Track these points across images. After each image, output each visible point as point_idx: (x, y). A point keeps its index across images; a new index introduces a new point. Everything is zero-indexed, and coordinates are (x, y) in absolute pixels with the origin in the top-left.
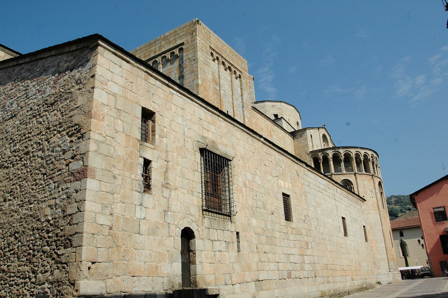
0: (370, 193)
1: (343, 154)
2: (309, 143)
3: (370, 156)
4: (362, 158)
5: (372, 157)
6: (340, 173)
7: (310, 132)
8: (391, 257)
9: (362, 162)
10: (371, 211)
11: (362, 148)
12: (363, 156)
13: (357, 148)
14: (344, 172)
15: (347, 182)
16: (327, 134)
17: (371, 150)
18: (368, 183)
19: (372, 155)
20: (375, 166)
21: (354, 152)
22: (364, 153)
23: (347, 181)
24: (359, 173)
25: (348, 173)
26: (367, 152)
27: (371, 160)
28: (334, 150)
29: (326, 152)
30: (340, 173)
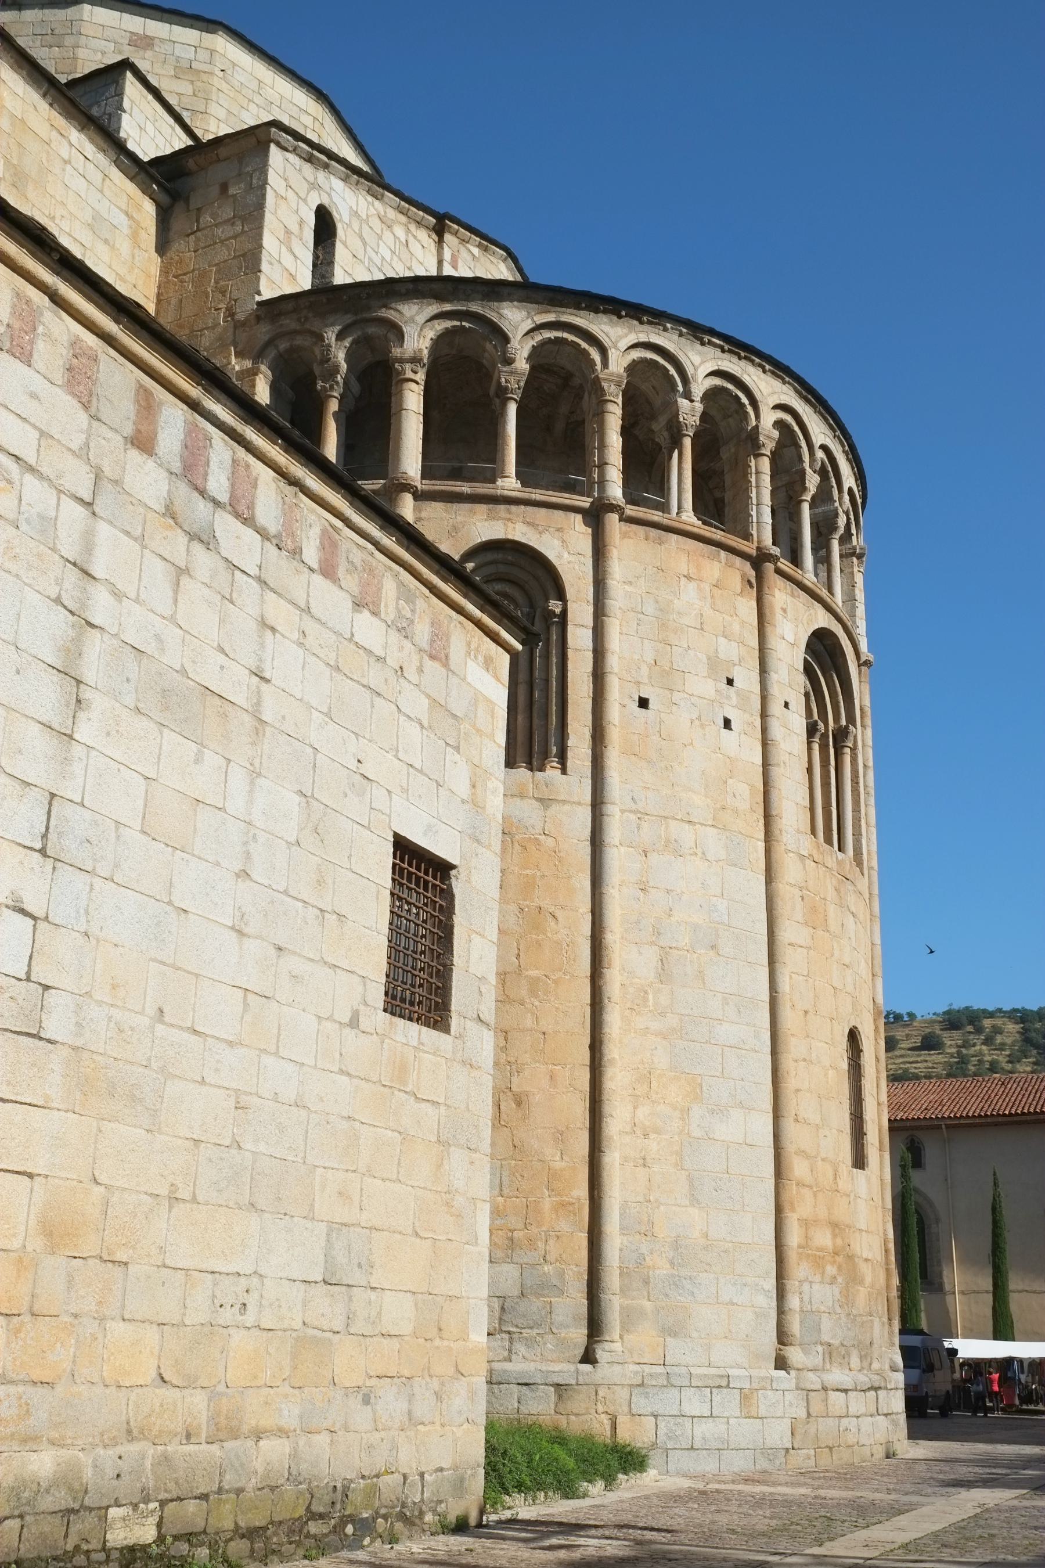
0: (709, 687)
1: (521, 351)
2: (269, 241)
7: (314, 186)
8: (824, 1239)
10: (686, 835)
11: (698, 331)
13: (657, 317)
14: (509, 483)
17: (781, 370)
18: (708, 611)
21: (624, 344)
22: (717, 381)
24: (631, 511)
25: (537, 495)
29: (384, 313)
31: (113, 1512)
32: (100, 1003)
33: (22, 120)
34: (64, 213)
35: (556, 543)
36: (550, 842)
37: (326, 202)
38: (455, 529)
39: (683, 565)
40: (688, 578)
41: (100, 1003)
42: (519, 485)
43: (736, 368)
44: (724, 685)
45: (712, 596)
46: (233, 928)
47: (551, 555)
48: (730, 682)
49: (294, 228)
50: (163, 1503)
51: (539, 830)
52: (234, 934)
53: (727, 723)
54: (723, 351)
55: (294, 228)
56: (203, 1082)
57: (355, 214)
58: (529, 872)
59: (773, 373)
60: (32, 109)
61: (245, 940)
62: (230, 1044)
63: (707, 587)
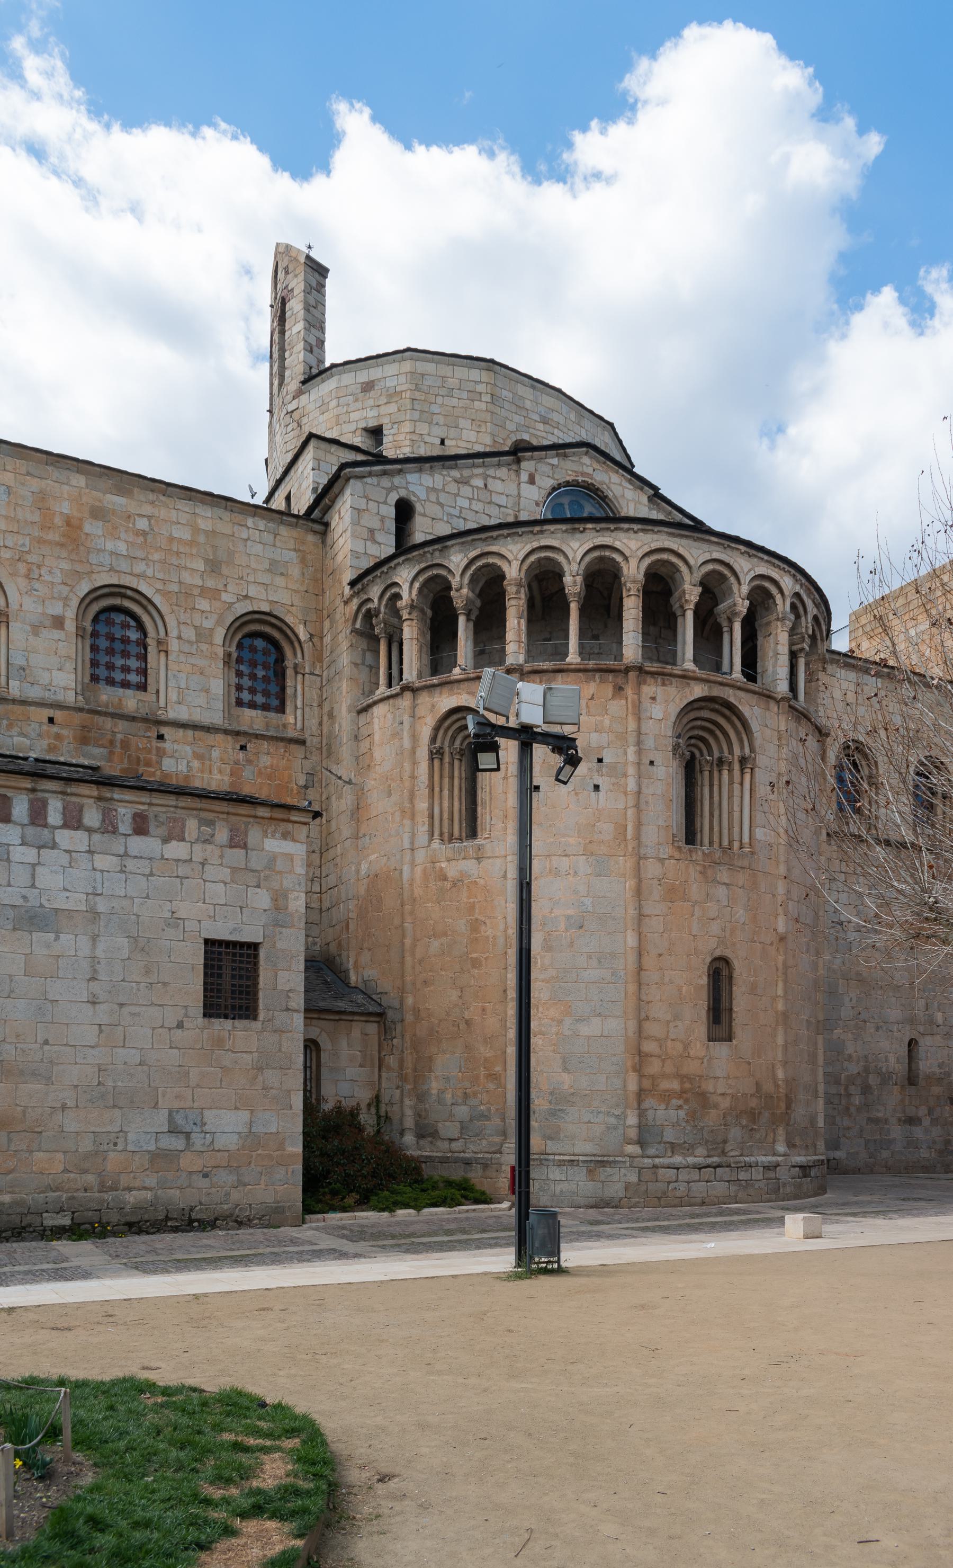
7: (394, 488)
26: (618, 544)
31: (45, 1215)
32: (10, 1043)
33: (213, 531)
34: (249, 571)
36: (481, 882)
37: (403, 493)
38: (433, 706)
41: (10, 1043)
43: (608, 539)
45: (588, 707)
46: (88, 1002)
48: (600, 760)
49: (376, 524)
50: (73, 1213)
51: (476, 875)
52: (89, 1005)
53: (597, 788)
54: (597, 531)
56: (76, 1063)
58: (472, 900)
59: (643, 530)
60: (219, 521)
61: (97, 1006)
62: (92, 1047)
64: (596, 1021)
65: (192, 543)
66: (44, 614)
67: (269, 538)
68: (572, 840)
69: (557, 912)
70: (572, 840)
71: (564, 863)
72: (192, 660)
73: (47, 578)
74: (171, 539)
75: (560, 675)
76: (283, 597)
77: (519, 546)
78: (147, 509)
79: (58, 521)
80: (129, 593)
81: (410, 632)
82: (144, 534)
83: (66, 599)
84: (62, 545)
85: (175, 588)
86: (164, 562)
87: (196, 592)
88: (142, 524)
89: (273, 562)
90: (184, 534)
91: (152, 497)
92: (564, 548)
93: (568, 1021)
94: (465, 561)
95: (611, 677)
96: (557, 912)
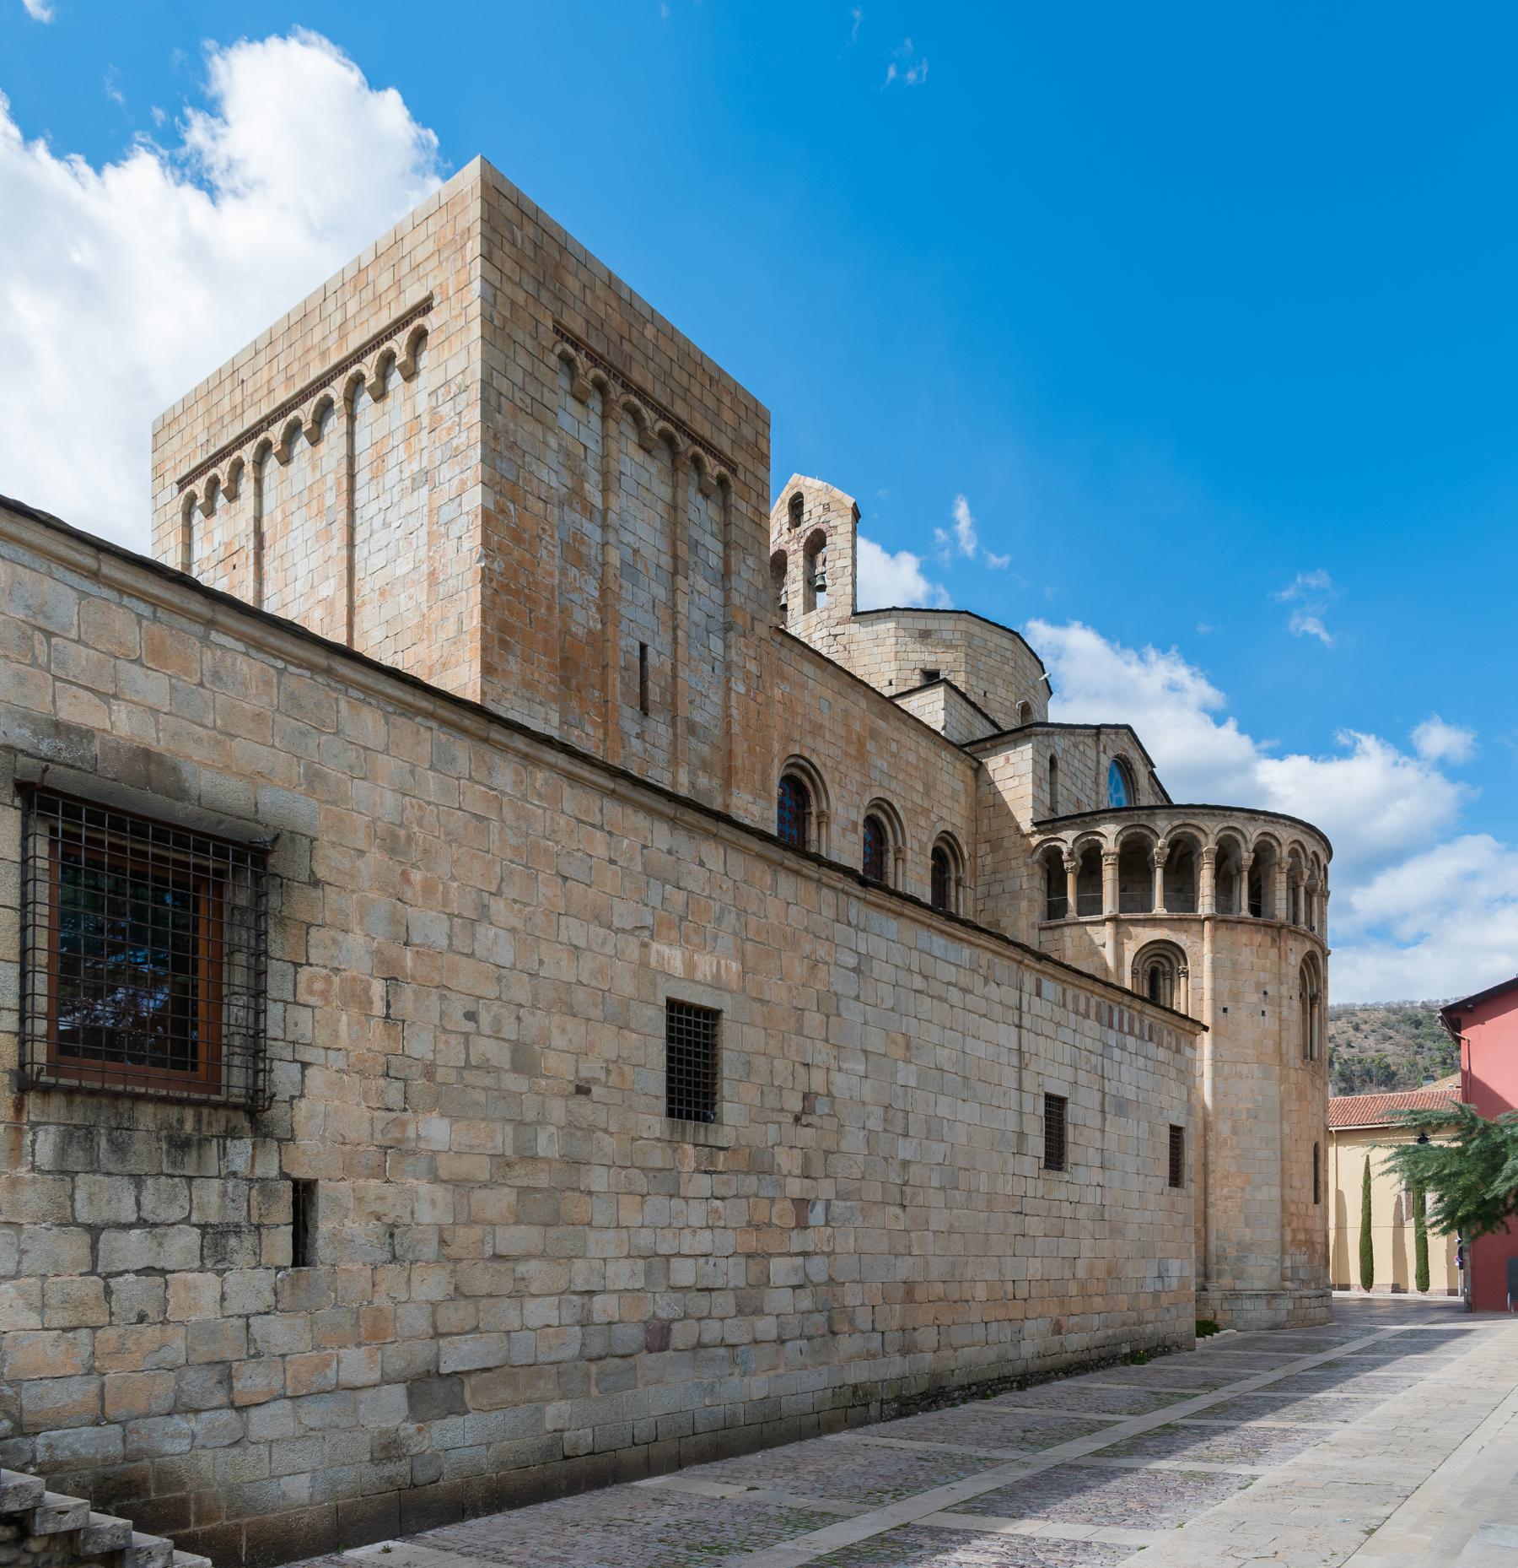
3: (1285, 851)
4: (1247, 857)
5: (1294, 853)
6: (1141, 916)
7: (1049, 746)
9: (1245, 874)
12: (1251, 847)
15: (1158, 951)
16: (1137, 756)
18: (1256, 960)
19: (1296, 846)
20: (1302, 890)
23: (1168, 947)
25: (1175, 915)
27: (1286, 866)
28: (1129, 824)
30: (1141, 916)
35: (1184, 937)
39: (1244, 939)
40: (1246, 945)
42: (1165, 911)
44: (1262, 995)
47: (1181, 945)
48: (1265, 993)
55: (1042, 776)
57: (1064, 750)
63: (1255, 948)
64: (1265, 1188)
65: (917, 768)
66: (848, 819)
67: (951, 768)
68: (1249, 1052)
69: (1241, 1106)
70: (1249, 1052)
71: (1245, 1069)
72: (918, 870)
73: (849, 787)
74: (908, 762)
75: (1239, 926)
76: (959, 821)
77: (1214, 823)
78: (896, 735)
79: (854, 737)
80: (886, 806)
81: (1109, 874)
82: (894, 755)
83: (859, 807)
84: (856, 759)
85: (909, 805)
86: (904, 782)
87: (919, 810)
88: (894, 747)
89: (954, 790)
90: (913, 759)
91: (898, 724)
92: (1245, 831)
93: (1248, 1189)
94: (1169, 828)
95: (1270, 931)
96: (1241, 1106)
